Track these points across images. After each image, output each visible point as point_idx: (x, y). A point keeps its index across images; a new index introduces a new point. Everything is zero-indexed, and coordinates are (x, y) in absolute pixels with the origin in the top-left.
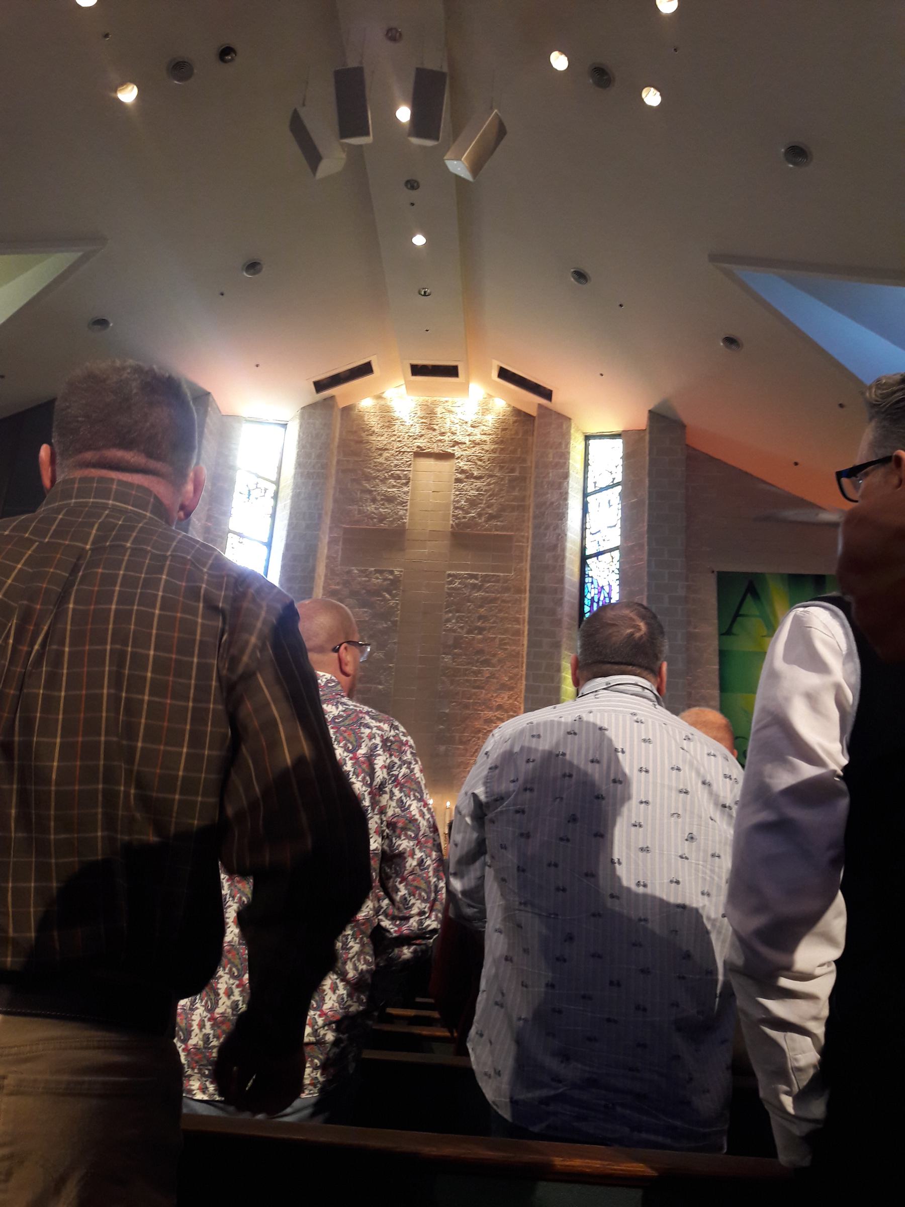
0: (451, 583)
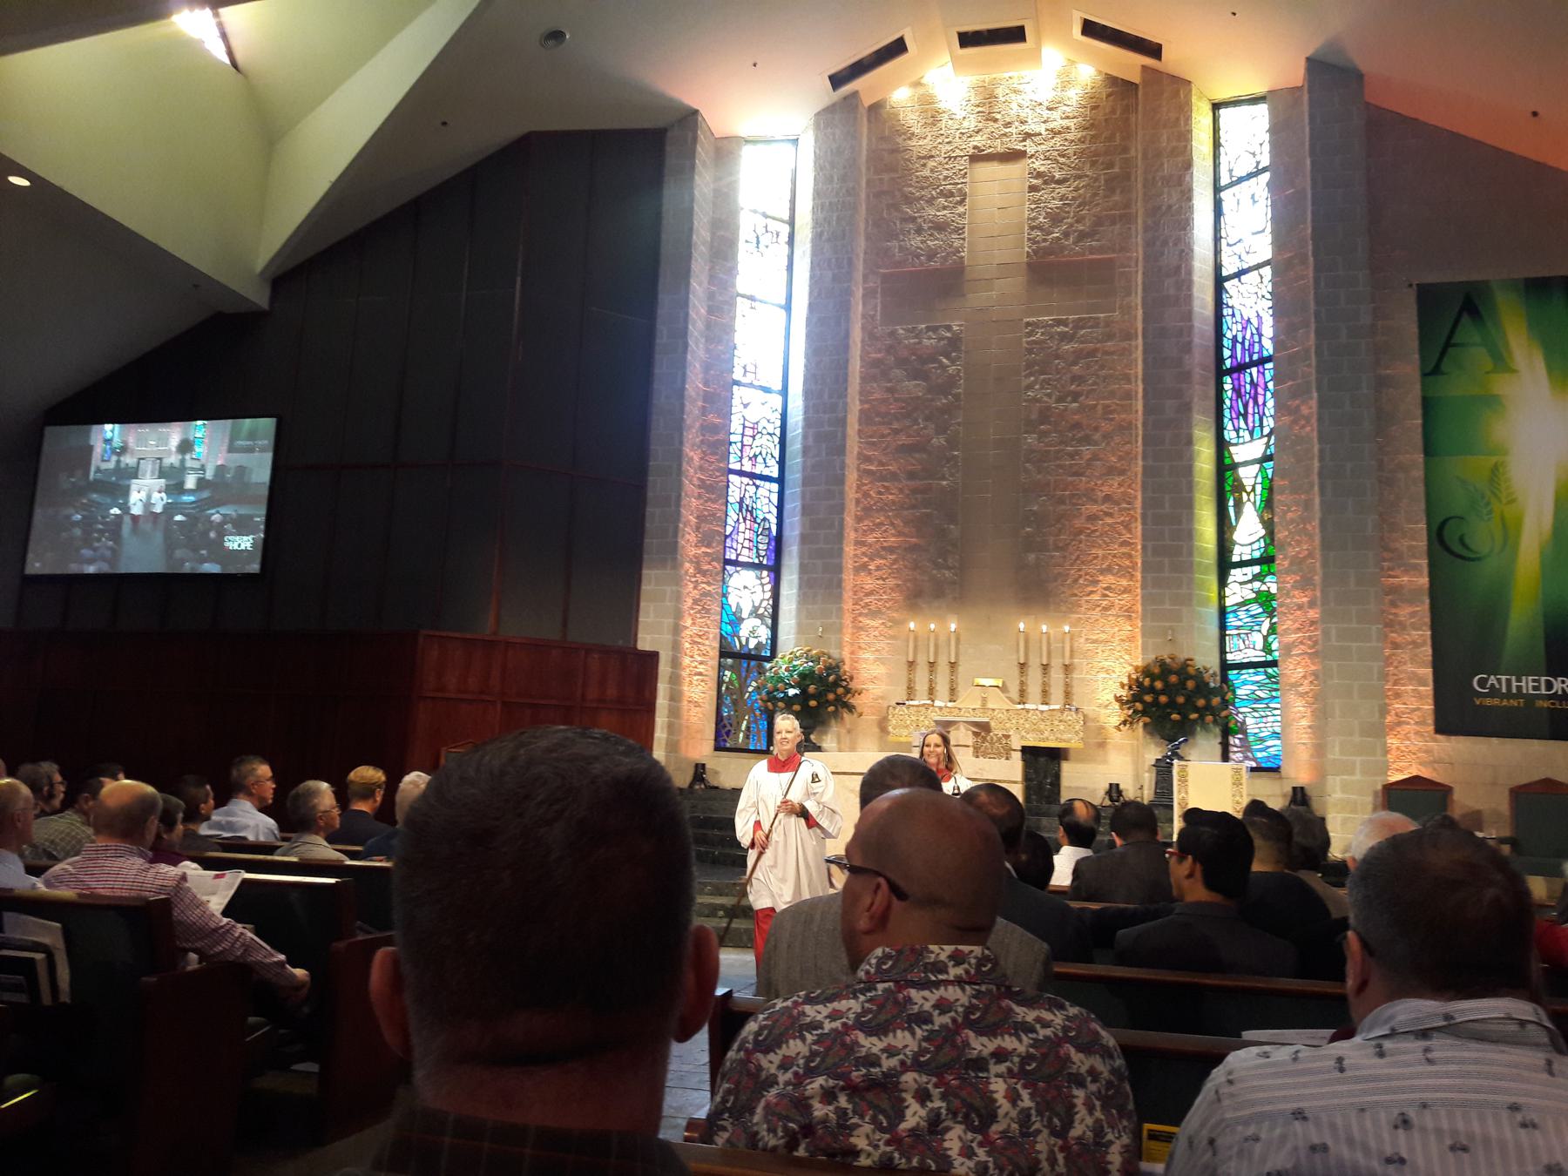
0: (1030, 334)
